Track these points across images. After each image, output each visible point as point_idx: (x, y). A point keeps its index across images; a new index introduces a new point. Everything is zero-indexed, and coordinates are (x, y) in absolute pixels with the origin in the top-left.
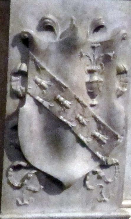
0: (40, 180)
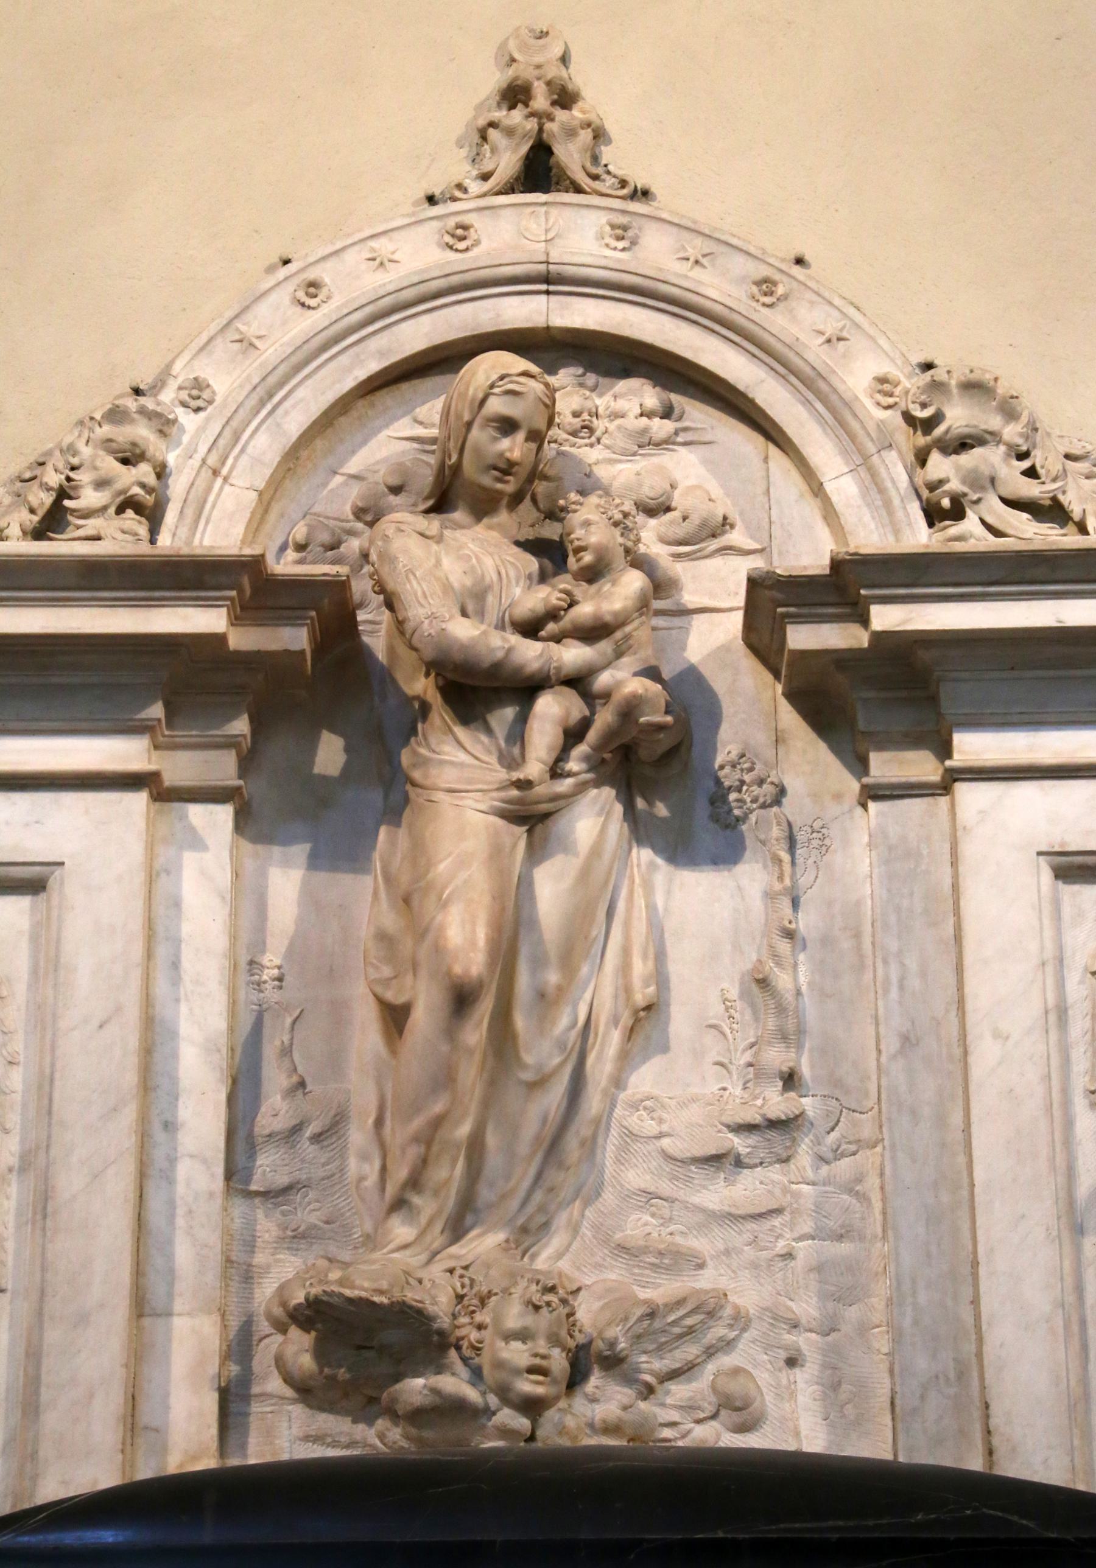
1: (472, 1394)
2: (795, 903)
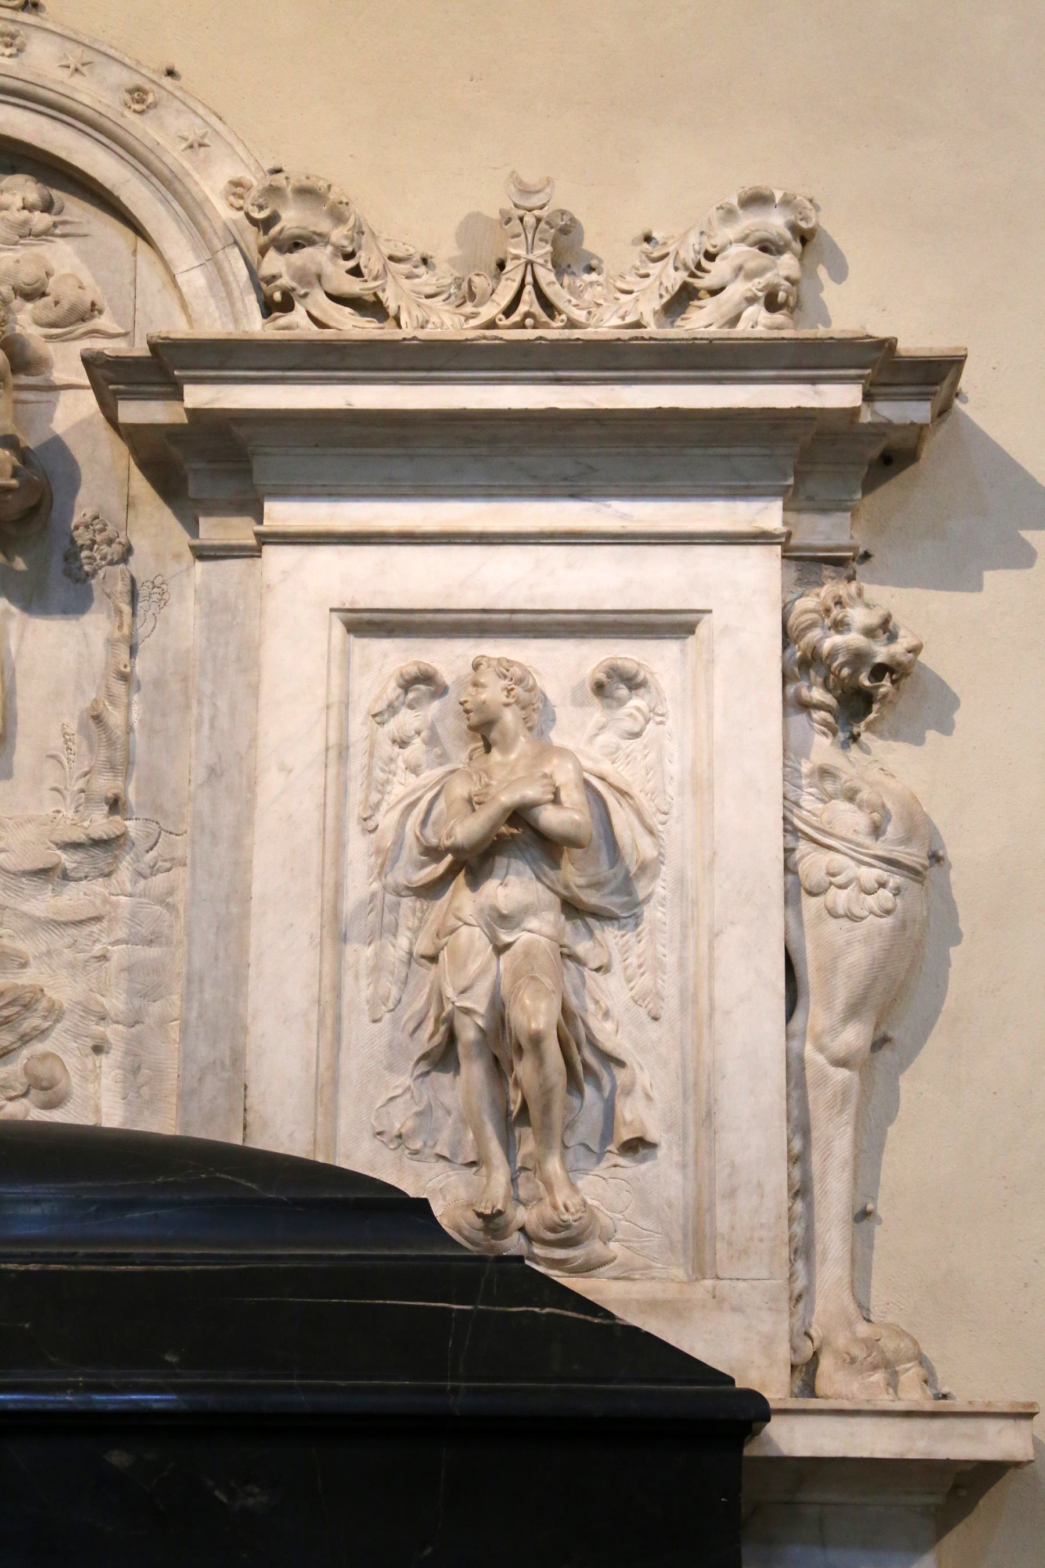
2: (133, 651)
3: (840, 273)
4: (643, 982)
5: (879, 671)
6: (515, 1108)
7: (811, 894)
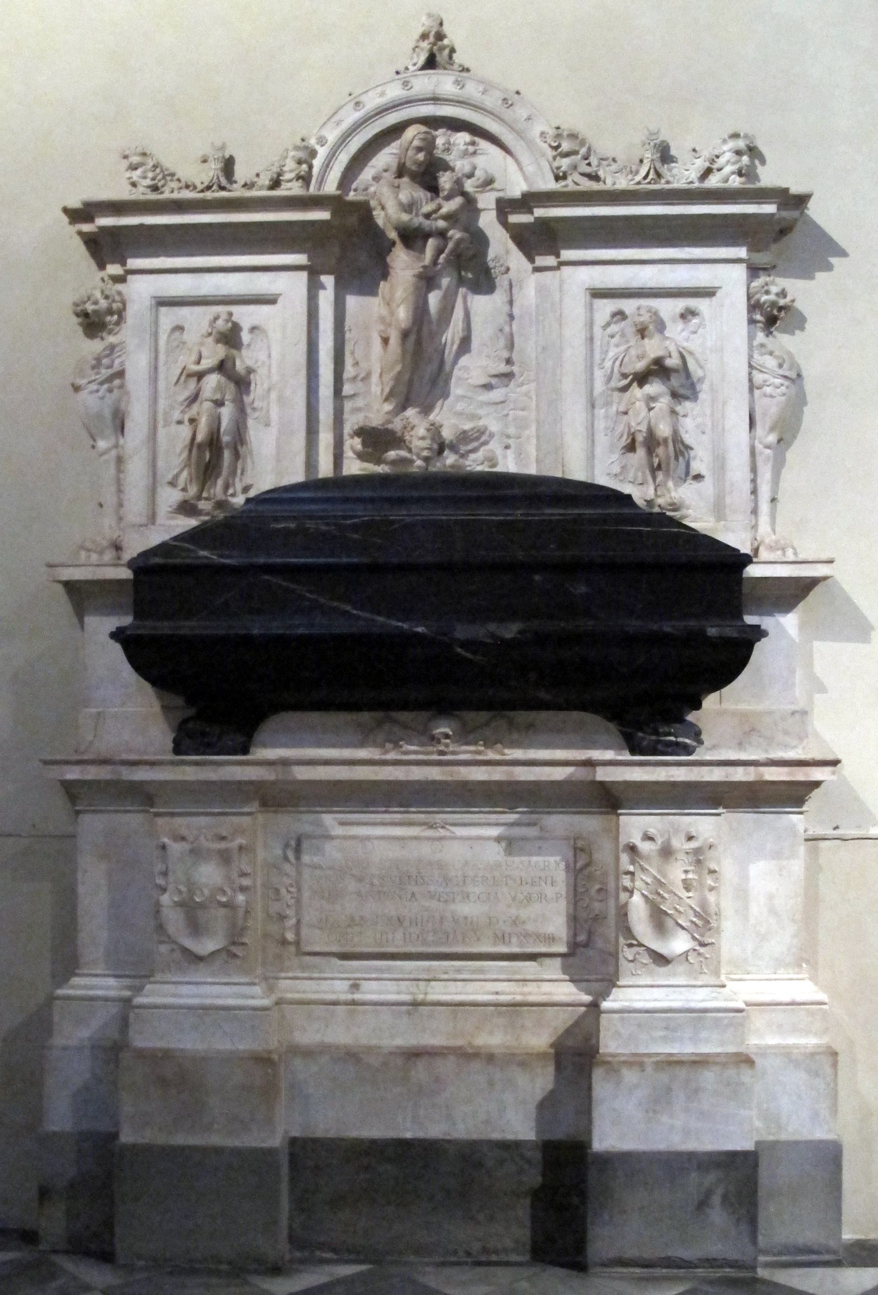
0: (649, 955)
1: (408, 455)
3: (763, 162)
4: (699, 420)
5: (781, 309)
6: (655, 465)
7: (758, 388)
